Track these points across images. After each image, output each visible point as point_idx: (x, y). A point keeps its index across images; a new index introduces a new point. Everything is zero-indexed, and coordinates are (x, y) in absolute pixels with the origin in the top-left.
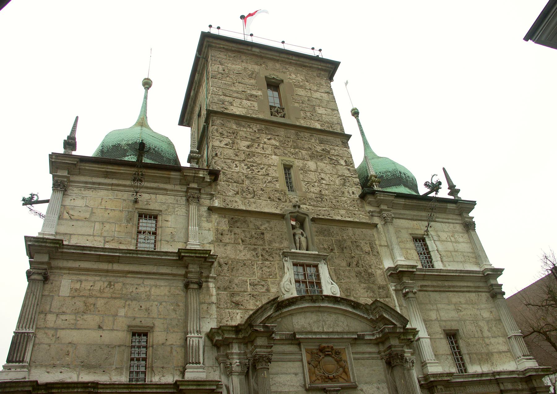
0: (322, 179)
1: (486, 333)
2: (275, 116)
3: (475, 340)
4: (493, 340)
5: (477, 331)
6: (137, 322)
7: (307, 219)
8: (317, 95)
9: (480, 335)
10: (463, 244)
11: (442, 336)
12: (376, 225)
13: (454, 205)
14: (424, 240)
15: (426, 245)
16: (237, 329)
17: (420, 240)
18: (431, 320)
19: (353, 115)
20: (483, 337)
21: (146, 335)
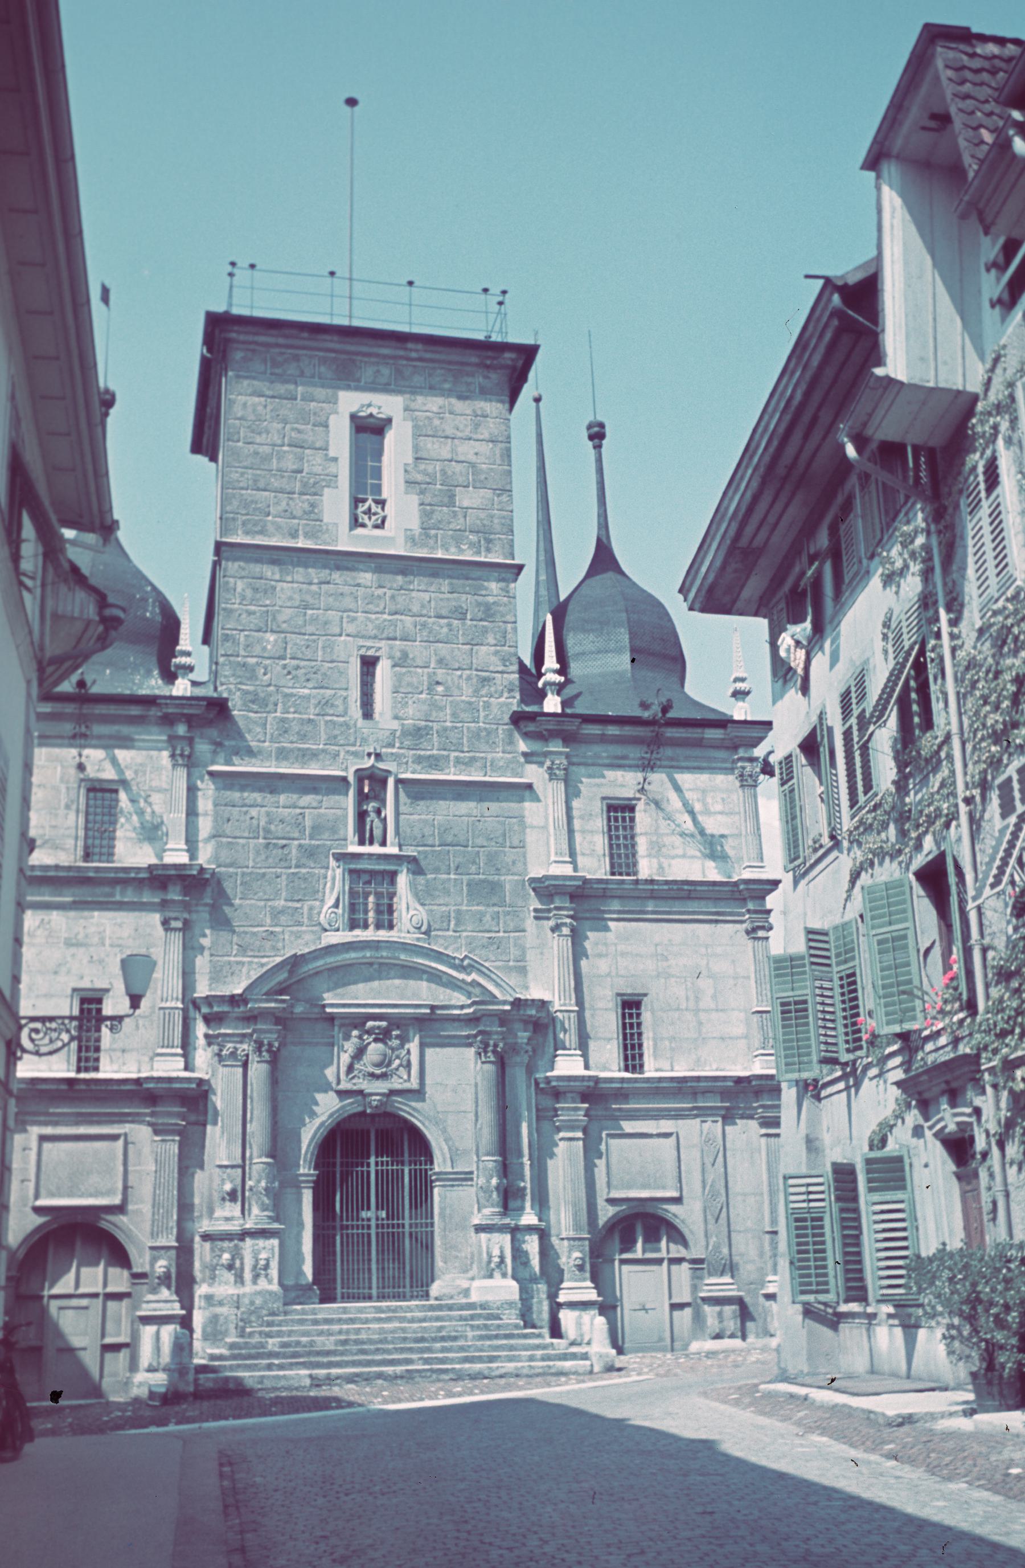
0: (438, 683)
1: (707, 1002)
2: (363, 525)
3: (676, 1015)
4: (714, 1015)
5: (687, 999)
6: (85, 984)
7: (391, 782)
8: (466, 450)
9: (692, 1004)
10: (719, 817)
11: (611, 1005)
12: (529, 786)
13: (721, 731)
14: (632, 809)
15: (632, 819)
16: (233, 1000)
17: (620, 812)
18: (599, 976)
19: (591, 438)
20: (697, 1011)
21: (99, 1001)
